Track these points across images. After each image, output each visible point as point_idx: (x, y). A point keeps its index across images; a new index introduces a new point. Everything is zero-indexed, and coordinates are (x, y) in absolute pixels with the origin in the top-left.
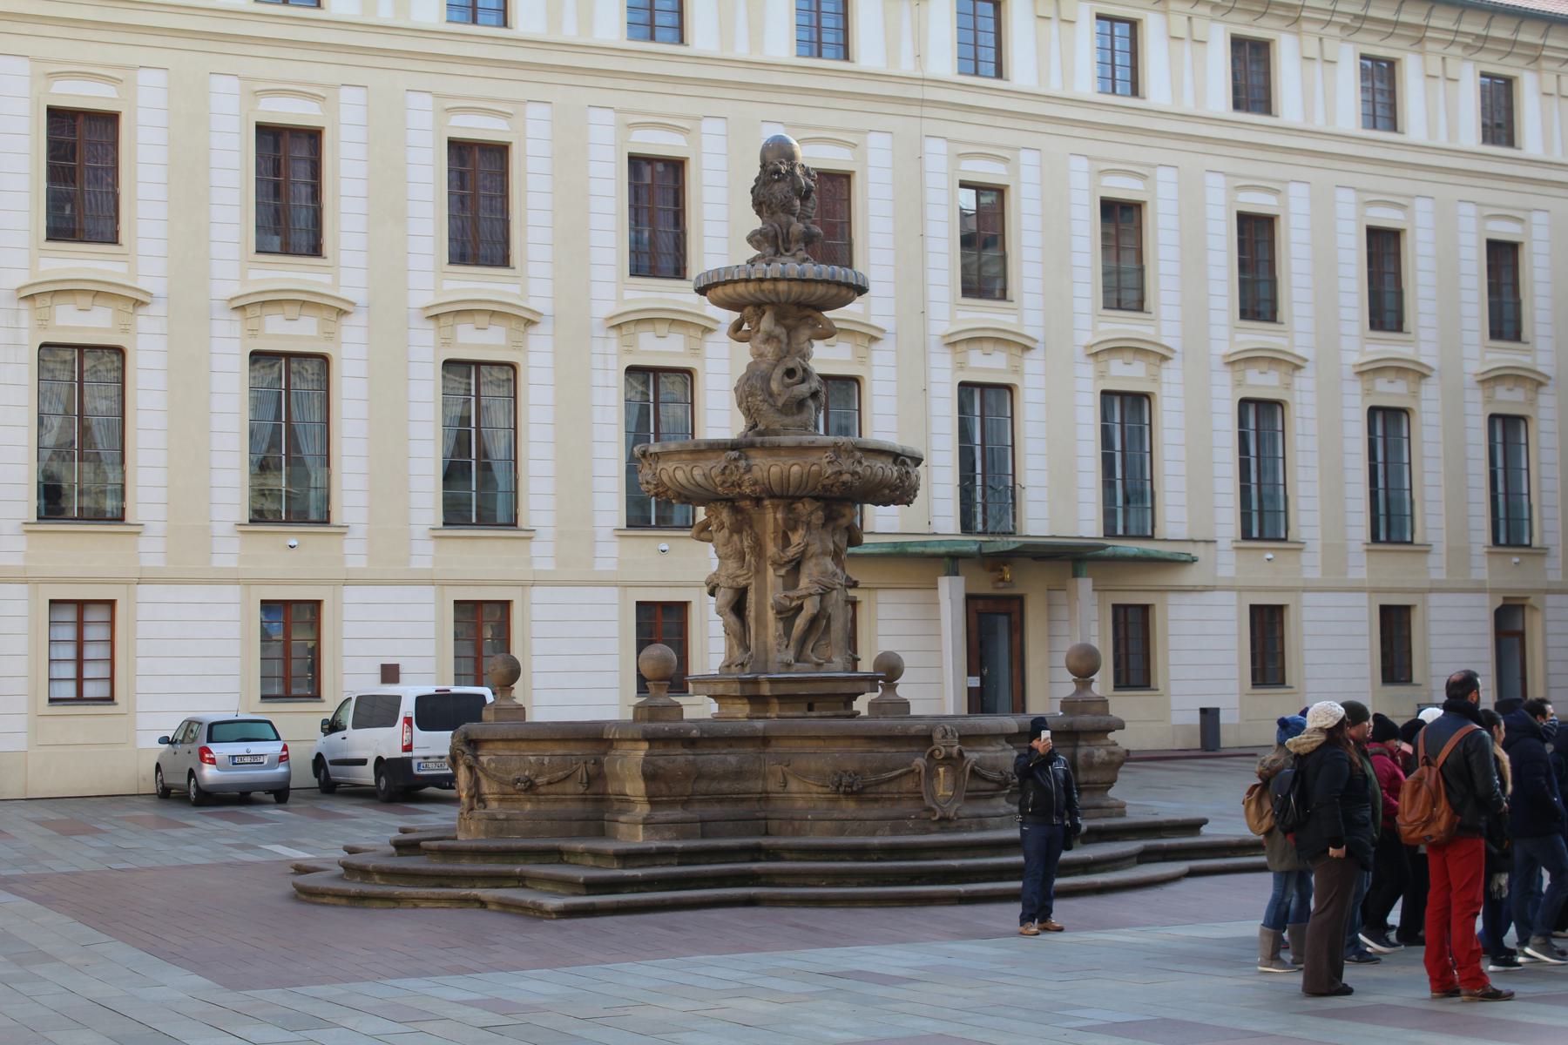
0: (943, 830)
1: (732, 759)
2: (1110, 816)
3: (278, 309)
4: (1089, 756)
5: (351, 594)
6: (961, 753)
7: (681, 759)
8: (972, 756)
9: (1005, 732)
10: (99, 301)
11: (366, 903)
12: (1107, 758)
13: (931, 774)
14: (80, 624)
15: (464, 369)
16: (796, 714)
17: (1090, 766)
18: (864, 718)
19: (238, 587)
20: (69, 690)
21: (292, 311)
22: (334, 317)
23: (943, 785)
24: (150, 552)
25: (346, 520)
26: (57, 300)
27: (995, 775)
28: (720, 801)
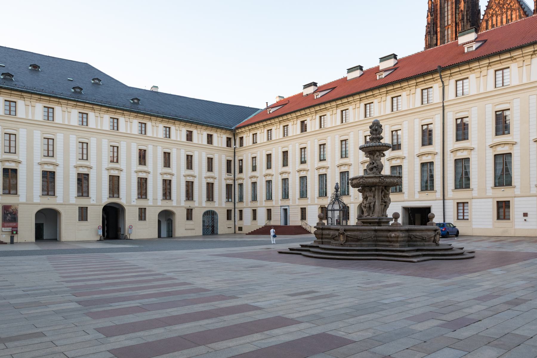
0: (342, 246)
1: (327, 232)
2: (395, 247)
3: (499, 146)
4: (391, 235)
5: (516, 199)
6: (344, 233)
7: (319, 232)
8: (346, 233)
9: (400, 229)
10: (464, 150)
11: (419, 256)
12: (394, 236)
13: (339, 236)
14: (463, 206)
15: (503, 155)
16: (367, 225)
17: (391, 237)
18: (402, 226)
19: (492, 199)
20: (462, 218)
21: (503, 146)
22: (512, 145)
23: (342, 238)
24: (475, 193)
25: (515, 185)
26: (457, 152)
27: (355, 237)
28: (328, 239)
